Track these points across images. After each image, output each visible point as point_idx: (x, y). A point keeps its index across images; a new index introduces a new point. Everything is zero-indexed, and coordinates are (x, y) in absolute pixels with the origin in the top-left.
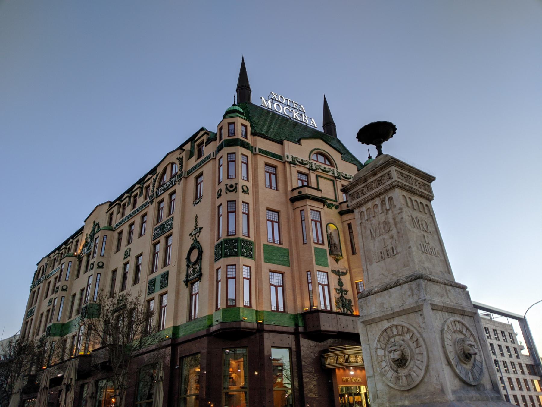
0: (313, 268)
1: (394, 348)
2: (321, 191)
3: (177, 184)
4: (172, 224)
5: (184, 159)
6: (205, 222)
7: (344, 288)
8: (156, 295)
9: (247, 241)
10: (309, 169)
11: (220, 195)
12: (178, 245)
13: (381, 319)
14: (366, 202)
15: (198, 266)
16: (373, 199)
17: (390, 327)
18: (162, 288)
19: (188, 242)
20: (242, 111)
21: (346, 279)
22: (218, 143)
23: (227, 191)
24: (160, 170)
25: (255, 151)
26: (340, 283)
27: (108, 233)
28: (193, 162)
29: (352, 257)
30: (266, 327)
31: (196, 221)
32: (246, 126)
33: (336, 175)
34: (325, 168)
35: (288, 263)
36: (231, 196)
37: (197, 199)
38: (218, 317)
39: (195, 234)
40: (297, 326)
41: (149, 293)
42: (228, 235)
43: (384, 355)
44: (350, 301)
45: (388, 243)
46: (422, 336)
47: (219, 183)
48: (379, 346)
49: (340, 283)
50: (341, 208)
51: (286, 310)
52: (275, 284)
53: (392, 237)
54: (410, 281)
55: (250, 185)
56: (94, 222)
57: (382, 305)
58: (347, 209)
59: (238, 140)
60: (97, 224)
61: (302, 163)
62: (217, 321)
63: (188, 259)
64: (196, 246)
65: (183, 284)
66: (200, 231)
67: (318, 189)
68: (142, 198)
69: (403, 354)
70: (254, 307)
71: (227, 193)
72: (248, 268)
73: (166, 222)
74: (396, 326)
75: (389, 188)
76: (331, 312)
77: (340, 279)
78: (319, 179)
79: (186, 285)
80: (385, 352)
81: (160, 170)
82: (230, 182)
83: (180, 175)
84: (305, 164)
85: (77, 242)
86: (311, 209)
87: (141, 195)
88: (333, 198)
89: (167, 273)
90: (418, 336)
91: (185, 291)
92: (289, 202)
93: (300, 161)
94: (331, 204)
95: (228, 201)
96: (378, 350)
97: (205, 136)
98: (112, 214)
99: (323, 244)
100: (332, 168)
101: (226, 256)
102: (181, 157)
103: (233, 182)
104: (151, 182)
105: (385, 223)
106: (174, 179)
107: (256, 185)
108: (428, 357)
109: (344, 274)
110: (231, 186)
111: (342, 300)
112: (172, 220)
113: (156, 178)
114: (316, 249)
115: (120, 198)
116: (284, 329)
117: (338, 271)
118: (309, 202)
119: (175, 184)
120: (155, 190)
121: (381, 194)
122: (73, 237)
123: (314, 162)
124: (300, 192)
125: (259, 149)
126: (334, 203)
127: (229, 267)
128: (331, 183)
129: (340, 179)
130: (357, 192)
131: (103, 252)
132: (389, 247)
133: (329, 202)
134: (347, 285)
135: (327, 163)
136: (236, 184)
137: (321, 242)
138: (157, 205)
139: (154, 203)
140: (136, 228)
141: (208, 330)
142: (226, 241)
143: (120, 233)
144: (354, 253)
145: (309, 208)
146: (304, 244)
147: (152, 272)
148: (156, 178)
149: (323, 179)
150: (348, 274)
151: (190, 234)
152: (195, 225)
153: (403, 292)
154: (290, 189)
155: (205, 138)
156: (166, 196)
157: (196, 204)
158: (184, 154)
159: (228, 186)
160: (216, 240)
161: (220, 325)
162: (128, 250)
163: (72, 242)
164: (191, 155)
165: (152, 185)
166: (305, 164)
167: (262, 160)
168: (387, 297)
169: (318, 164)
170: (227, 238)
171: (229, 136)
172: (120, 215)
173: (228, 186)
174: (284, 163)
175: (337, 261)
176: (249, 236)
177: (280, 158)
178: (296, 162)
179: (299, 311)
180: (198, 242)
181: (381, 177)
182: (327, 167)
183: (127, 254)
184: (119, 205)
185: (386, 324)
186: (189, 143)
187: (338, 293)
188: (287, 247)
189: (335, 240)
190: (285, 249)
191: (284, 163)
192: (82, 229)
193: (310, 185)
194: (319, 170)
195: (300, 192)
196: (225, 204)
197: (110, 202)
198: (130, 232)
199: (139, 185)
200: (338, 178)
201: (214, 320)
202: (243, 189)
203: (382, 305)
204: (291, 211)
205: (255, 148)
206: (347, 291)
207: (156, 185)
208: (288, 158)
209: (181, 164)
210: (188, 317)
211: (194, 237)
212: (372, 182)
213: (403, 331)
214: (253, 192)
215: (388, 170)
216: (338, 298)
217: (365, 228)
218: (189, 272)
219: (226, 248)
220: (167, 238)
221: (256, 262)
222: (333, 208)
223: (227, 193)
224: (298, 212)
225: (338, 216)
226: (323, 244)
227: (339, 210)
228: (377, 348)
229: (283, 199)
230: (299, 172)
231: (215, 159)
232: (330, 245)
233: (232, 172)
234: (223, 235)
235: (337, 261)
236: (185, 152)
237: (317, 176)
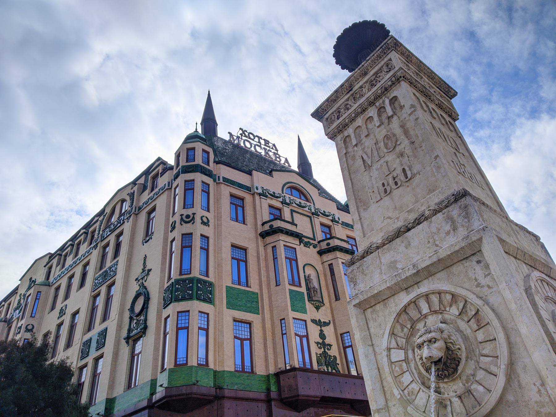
0: (288, 315)
1: (430, 336)
2: (296, 225)
3: (126, 222)
4: (116, 269)
5: (136, 193)
6: (154, 264)
7: (327, 341)
8: (90, 360)
9: (205, 282)
10: (282, 203)
11: (173, 228)
12: (121, 295)
13: (394, 291)
14: (353, 120)
15: (142, 318)
16: (364, 111)
17: (414, 302)
18: (98, 349)
19: (134, 288)
20: (204, 137)
21: (329, 331)
22: (175, 171)
23: (182, 223)
25: (219, 180)
26: (322, 336)
27: (44, 289)
28: (146, 196)
29: (335, 304)
30: (227, 393)
32: (208, 153)
33: (313, 210)
34: (300, 203)
35: (256, 311)
36: (187, 228)
37: (148, 235)
38: (163, 379)
39: (142, 279)
40: (268, 389)
41: (82, 358)
42: (181, 274)
43: (406, 360)
45: (395, 166)
46: (487, 303)
47: (174, 213)
48: (393, 344)
49: (322, 336)
50: (320, 246)
51: (254, 369)
52: (241, 337)
53: (402, 155)
54: (446, 207)
55: (210, 216)
56: (31, 279)
57: (392, 265)
58: (327, 247)
59: (198, 166)
60: (33, 281)
61: (274, 196)
62: (161, 386)
63: (132, 309)
64: (144, 294)
65: (123, 342)
66: (148, 274)
67: (293, 223)
68: (86, 244)
69: (448, 348)
70: (211, 366)
71: (182, 225)
72: (206, 316)
73: (110, 268)
74: (427, 296)
75: (390, 83)
76: (311, 371)
77: (321, 331)
78: (294, 214)
79: (127, 343)
80: (406, 354)
81: (108, 211)
82: (185, 212)
83: (130, 212)
84: (277, 197)
85: (9, 304)
87: (84, 242)
88: (311, 236)
89: (106, 330)
90: (479, 302)
91: (125, 350)
92: (259, 237)
93: (272, 193)
94: (308, 242)
95: (183, 235)
96: (392, 351)
97: (161, 166)
98: (50, 268)
99: (300, 286)
100: (308, 204)
101: (177, 300)
102: (132, 192)
103: (190, 212)
104: (98, 224)
105: (387, 137)
106: (122, 217)
107: (218, 217)
108: (509, 343)
109: (326, 324)
110: (188, 216)
111: (325, 357)
112: (117, 265)
113: (104, 219)
114: (291, 291)
115: (62, 248)
116: (251, 395)
117: (319, 320)
119: (124, 223)
120: (101, 232)
122: (5, 300)
123: (287, 196)
124: (271, 226)
125: (223, 178)
126: (312, 241)
127: (180, 314)
128: (308, 219)
129: (318, 215)
131: (34, 312)
132: (399, 171)
133: (306, 240)
134: (331, 338)
135: (303, 197)
136: (194, 214)
137: (297, 283)
138: (101, 250)
139: (98, 247)
140: (76, 281)
141: (150, 400)
142: (177, 282)
143: (58, 288)
144: (337, 298)
145: (282, 243)
146: (277, 286)
147: (89, 330)
148: (104, 219)
150: (332, 324)
151: (136, 280)
152: (142, 267)
153: (434, 230)
154: (259, 223)
155: (160, 168)
156: (112, 239)
157: (146, 242)
158: (135, 188)
160: (166, 282)
161: (164, 392)
162: (64, 308)
163: (4, 305)
164: (144, 188)
165: (98, 227)
166: (277, 197)
167: (226, 190)
168: (402, 248)
169: (292, 198)
170: (179, 277)
171: (187, 162)
172: (59, 267)
173: (184, 217)
174: (253, 194)
175: (318, 308)
176: (207, 276)
177: (248, 189)
178: (267, 194)
179: (272, 370)
180: (145, 288)
182: (303, 202)
183: (62, 312)
184: (61, 255)
185: (404, 299)
186: (144, 177)
187: (320, 348)
189: (315, 284)
190: (253, 293)
191: (253, 194)
192: (17, 288)
193: (283, 218)
194: (294, 205)
195: (271, 226)
196: (178, 239)
197: (50, 253)
198: (69, 286)
199: (84, 230)
200: (316, 214)
201: (158, 384)
202: (202, 219)
203: (392, 265)
204: (261, 249)
205: (219, 177)
206: (330, 346)
207: (102, 227)
208: (257, 189)
209: (132, 200)
210: (127, 385)
211: (141, 281)
212: (361, 87)
213: (443, 301)
214: (215, 225)
216: (320, 354)
217: (354, 158)
218: (132, 327)
219: (177, 290)
220: (110, 287)
221: (216, 308)
222: (311, 247)
223: (182, 225)
225: (317, 256)
226: (300, 286)
227: (318, 249)
228: (389, 349)
229: (252, 235)
230: (271, 206)
231: (171, 188)
232: (308, 289)
233: (189, 201)
234: (175, 275)
235: (318, 308)
236: (137, 186)
237: (292, 211)
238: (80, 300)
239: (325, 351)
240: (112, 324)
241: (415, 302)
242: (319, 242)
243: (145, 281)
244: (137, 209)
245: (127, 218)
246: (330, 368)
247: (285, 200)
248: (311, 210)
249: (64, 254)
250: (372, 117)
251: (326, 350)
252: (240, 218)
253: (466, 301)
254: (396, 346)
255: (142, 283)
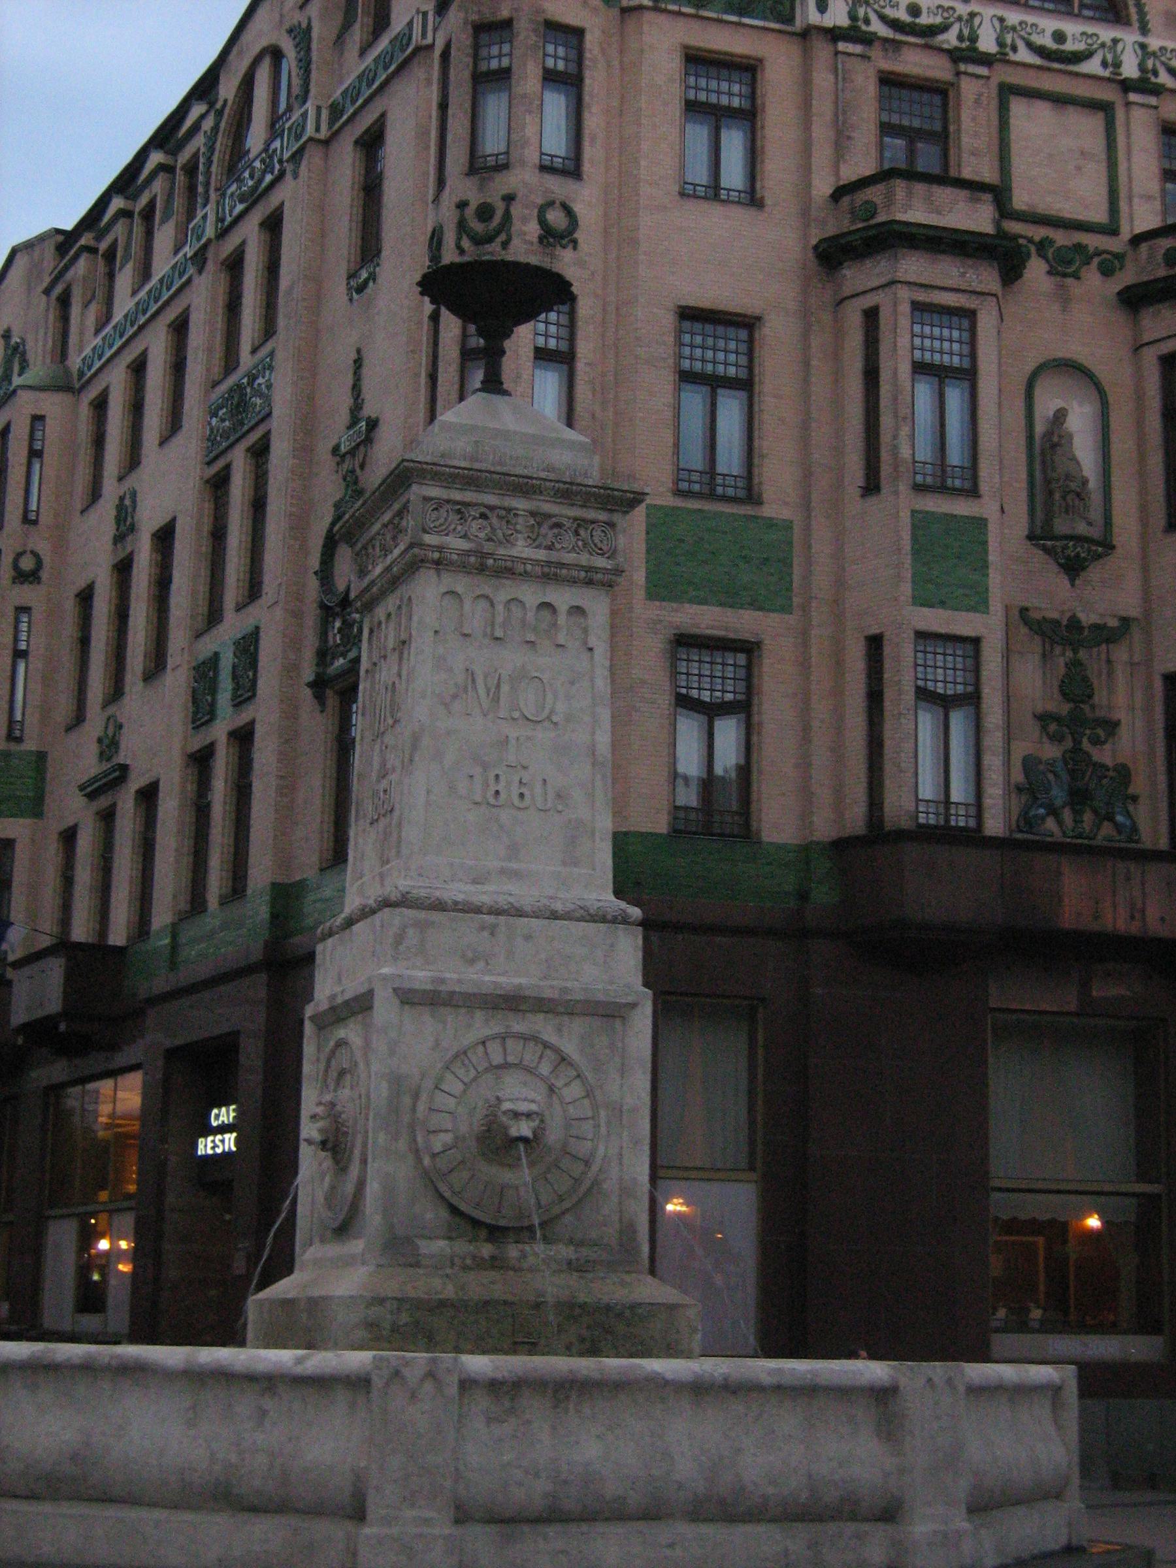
3: (289, 176)
4: (269, 387)
8: (219, 731)
24: (227, 89)
31: (356, 389)
33: (1130, 70)
34: (1059, 37)
35: (776, 596)
39: (352, 452)
40: (803, 896)
44: (1124, 774)
56: (7, 335)
60: (16, 348)
76: (973, 838)
78: (1018, 107)
79: (320, 698)
81: (227, 89)
86: (917, 306)
88: (1098, 214)
91: (316, 726)
98: (64, 301)
99: (973, 492)
100: (1106, 33)
104: (199, 141)
112: (271, 368)
114: (921, 521)
115: (92, 219)
118: (913, 266)
119: (282, 174)
126: (1092, 241)
133: (1061, 238)
136: (509, 199)
139: (210, 266)
148: (216, 129)
149: (1043, 110)
151: (335, 450)
154: (823, 187)
159: (470, 212)
173: (470, 212)
175: (1073, 568)
187: (1056, 738)
188: (785, 514)
190: (771, 524)
194: (1023, 55)
197: (58, 231)
202: (542, 222)
218: (331, 642)
224: (853, 317)
230: (889, 81)
238: (168, 485)
239: (1077, 749)
240: (269, 618)
242: (1137, 240)
243: (362, 466)
244: (325, 114)
245: (293, 156)
246: (1088, 817)
247: (974, 39)
248: (1117, 65)
249: (103, 246)
251: (1085, 744)
252: (733, 175)
255: (353, 471)
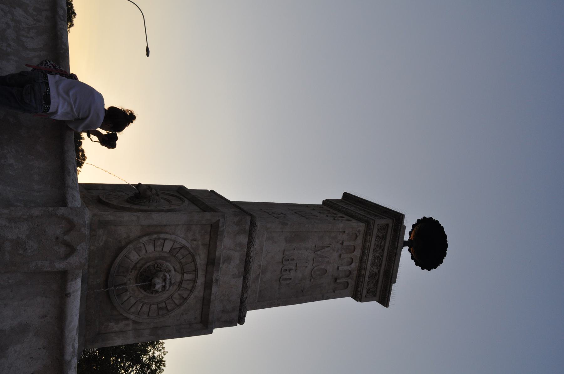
17: (196, 270)
48: (177, 246)
74: (194, 281)
80: (166, 252)
121: (359, 276)
130: (384, 238)
181: (377, 281)
215: (378, 293)
241: (195, 271)
250: (351, 264)
253: (178, 306)
254: (174, 247)
